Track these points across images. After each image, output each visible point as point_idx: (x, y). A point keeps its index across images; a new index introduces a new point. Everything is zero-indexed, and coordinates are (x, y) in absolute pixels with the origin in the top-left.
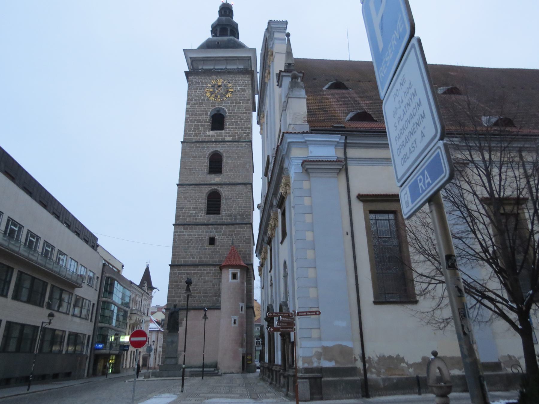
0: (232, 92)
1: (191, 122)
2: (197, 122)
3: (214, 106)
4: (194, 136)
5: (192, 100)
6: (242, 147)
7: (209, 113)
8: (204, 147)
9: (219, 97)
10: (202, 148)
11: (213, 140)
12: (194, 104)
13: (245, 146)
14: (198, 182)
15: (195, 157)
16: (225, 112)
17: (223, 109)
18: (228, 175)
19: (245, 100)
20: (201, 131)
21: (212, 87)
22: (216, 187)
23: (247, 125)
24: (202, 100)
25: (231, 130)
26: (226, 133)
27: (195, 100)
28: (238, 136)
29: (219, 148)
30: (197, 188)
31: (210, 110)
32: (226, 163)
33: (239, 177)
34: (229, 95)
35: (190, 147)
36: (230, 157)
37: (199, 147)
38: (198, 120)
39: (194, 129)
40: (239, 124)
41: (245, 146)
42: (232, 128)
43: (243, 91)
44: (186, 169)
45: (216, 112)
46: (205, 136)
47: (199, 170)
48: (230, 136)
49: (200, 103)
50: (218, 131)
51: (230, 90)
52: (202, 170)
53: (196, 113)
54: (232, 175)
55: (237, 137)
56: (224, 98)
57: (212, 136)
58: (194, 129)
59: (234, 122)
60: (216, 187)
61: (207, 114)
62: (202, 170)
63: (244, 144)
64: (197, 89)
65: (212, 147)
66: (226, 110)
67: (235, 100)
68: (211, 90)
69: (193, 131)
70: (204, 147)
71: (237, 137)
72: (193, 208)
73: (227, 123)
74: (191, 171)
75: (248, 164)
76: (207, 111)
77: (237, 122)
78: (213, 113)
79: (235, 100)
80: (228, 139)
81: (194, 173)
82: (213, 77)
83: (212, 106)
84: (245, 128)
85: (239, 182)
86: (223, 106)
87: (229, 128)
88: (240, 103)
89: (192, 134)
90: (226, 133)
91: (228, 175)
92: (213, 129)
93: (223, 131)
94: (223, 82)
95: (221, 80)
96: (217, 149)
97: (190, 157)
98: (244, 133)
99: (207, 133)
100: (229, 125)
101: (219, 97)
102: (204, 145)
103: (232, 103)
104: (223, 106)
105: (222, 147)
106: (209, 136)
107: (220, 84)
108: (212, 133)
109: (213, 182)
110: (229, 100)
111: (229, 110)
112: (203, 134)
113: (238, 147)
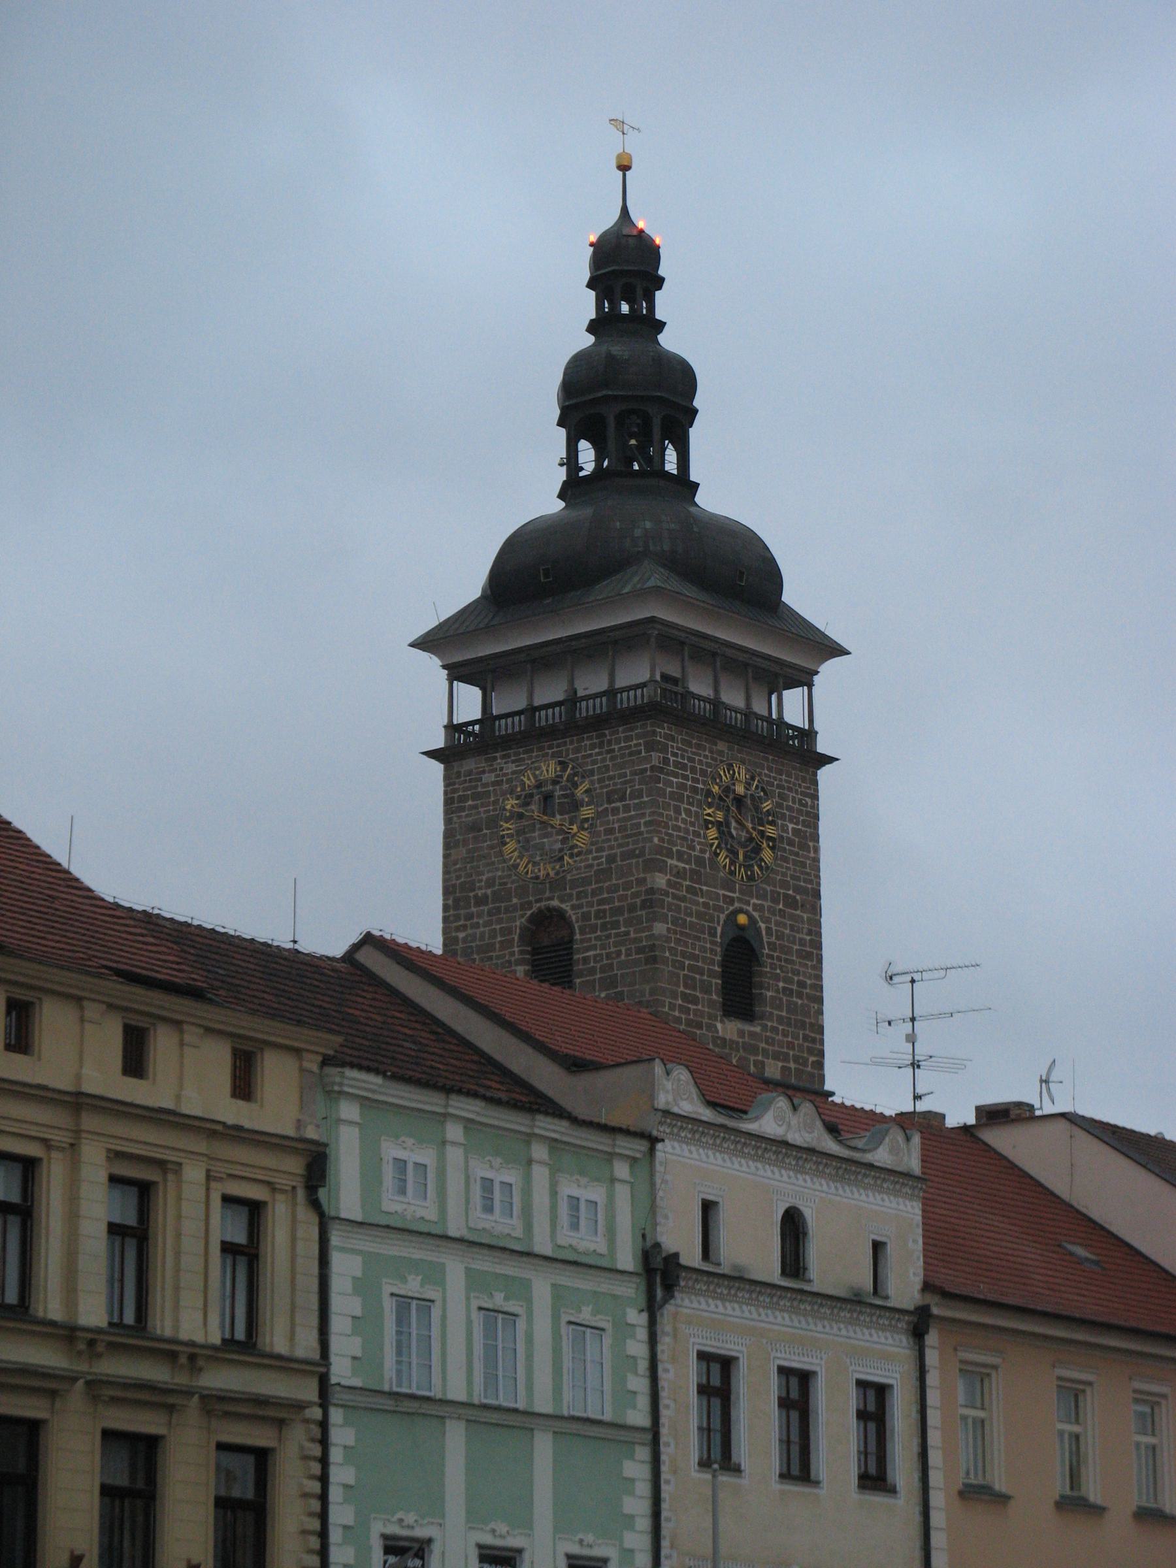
2: (692, 968)
3: (731, 901)
9: (741, 857)
27: (680, 856)
28: (796, 1059)
31: (722, 917)
42: (780, 1019)
48: (776, 1056)
50: (747, 1027)
51: (771, 831)
55: (792, 1065)
58: (685, 997)
66: (763, 926)
68: (720, 816)
71: (792, 1065)
82: (721, 746)
94: (748, 785)
98: (811, 1051)
99: (719, 1026)
103: (775, 901)
107: (740, 789)
108: (729, 1029)
111: (768, 929)
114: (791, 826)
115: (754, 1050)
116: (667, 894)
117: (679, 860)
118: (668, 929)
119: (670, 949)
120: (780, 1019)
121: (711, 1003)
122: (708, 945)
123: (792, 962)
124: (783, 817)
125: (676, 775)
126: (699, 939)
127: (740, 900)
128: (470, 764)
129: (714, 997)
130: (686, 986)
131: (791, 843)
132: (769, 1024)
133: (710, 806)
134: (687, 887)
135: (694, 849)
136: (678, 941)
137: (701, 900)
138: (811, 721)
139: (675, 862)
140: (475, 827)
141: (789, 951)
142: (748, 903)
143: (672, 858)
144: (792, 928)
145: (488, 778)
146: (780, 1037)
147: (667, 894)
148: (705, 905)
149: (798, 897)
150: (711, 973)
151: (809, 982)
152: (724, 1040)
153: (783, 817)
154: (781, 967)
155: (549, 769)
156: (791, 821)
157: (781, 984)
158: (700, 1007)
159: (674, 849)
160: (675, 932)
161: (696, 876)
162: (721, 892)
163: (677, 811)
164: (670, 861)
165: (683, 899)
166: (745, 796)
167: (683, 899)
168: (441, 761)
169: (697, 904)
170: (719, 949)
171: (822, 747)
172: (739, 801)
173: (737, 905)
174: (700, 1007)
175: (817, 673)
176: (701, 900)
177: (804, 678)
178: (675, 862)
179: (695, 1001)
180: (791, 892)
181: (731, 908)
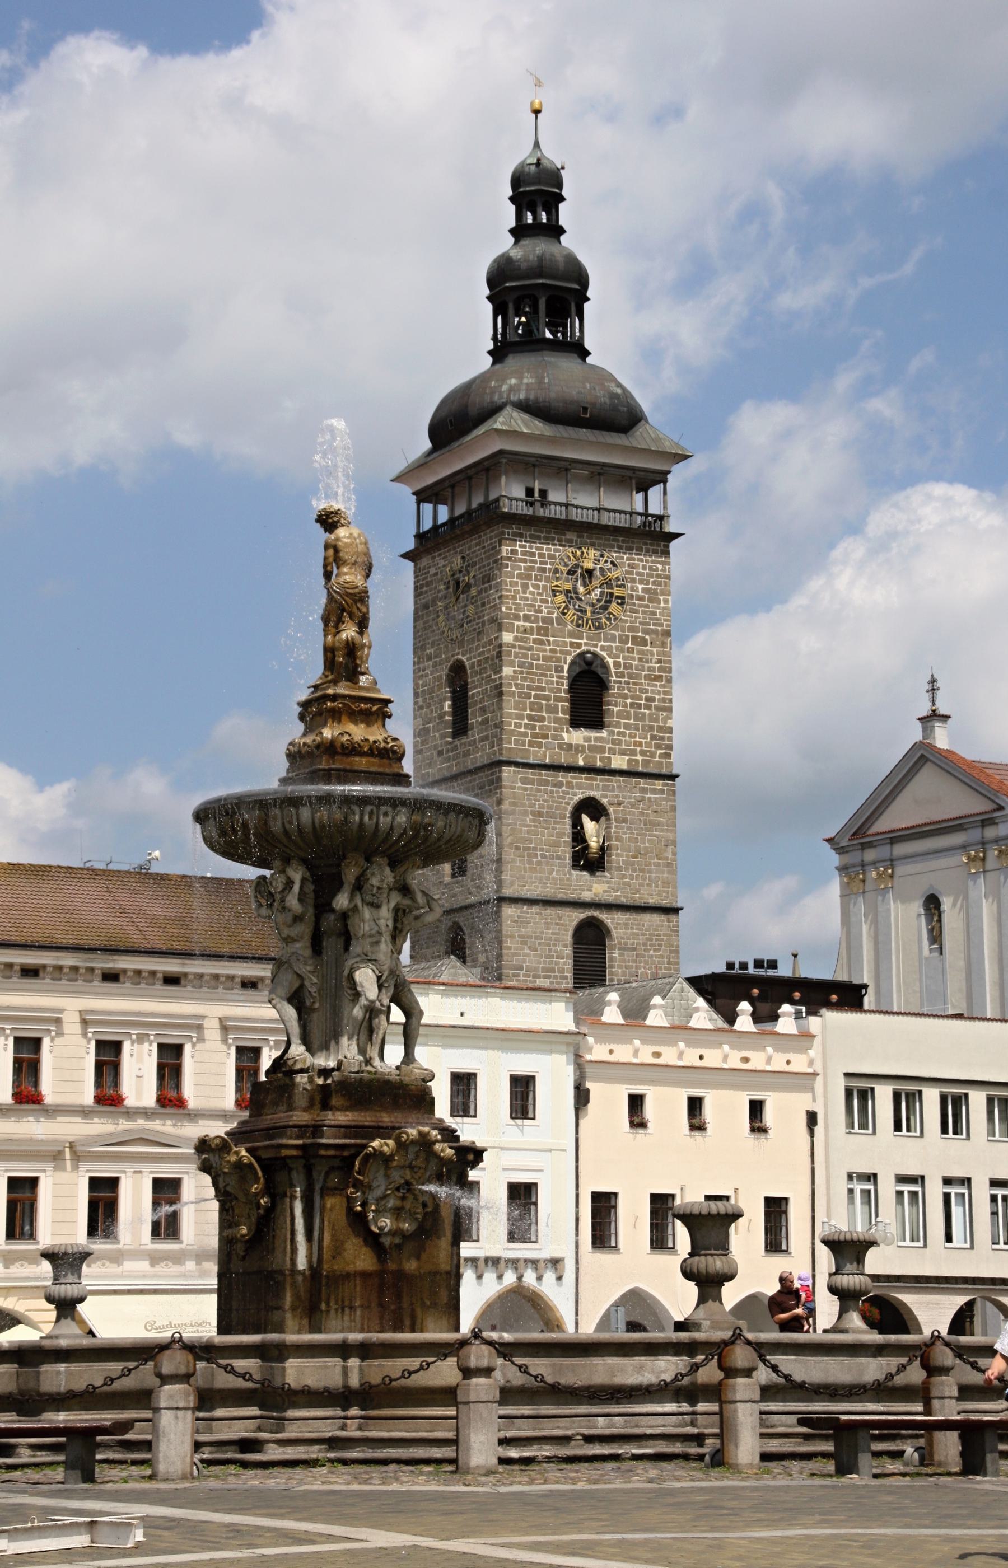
0: (623, 598)
1: (520, 695)
2: (536, 697)
3: (579, 646)
4: (531, 744)
5: (517, 618)
6: (654, 791)
7: (566, 667)
8: (560, 785)
9: (589, 614)
10: (555, 785)
11: (581, 763)
12: (525, 631)
13: (662, 791)
14: (549, 891)
15: (540, 814)
16: (605, 666)
17: (602, 659)
18: (624, 876)
19: (656, 632)
20: (548, 728)
21: (569, 573)
22: (596, 914)
23: (665, 721)
24: (545, 620)
25: (623, 734)
26: (614, 742)
27: (527, 618)
28: (643, 753)
29: (597, 789)
30: (549, 911)
31: (569, 659)
32: (618, 839)
33: (649, 885)
34: (614, 607)
35: (524, 781)
36: (625, 821)
37: (546, 783)
38: (539, 688)
39: (530, 718)
40: (644, 714)
41: (662, 791)
42: (627, 726)
43: (650, 600)
44: (517, 848)
45: (586, 668)
46: (560, 746)
47: (552, 857)
48: (622, 753)
49: (539, 628)
50: (593, 734)
51: (617, 591)
52: (559, 858)
53: (531, 665)
54: (631, 877)
55: (639, 758)
56: (604, 620)
57: (578, 749)
58: (530, 718)
59: (632, 705)
60: (596, 914)
61: (559, 670)
62: (559, 858)
63: (659, 784)
64: (529, 577)
65: (579, 786)
67: (631, 629)
68: (568, 586)
69: (526, 726)
70: (560, 785)
71: (639, 758)
72: (544, 970)
73: (614, 707)
74: (530, 856)
75: (670, 849)
76: (559, 660)
77: (639, 706)
78: (578, 670)
79: (631, 629)
80: (619, 762)
81: (539, 863)
83: (572, 644)
84: (661, 729)
85: (652, 901)
86: (603, 648)
87: (618, 725)
88: (644, 642)
89: (525, 735)
90: (614, 742)
91: (624, 876)
92: (576, 723)
93: (604, 734)
95: (592, 552)
96: (593, 793)
97: (525, 813)
99: (565, 735)
100: (620, 715)
101: (589, 614)
102: (561, 777)
103: (624, 640)
104: (603, 648)
105: (606, 788)
106: (570, 746)
107: (589, 564)
108: (577, 737)
109: (587, 896)
110: (616, 628)
111: (617, 665)
112: (555, 737)
113: (644, 791)
114: (640, 587)
115: (602, 750)
116: (514, 646)
117: (525, 621)
118: (515, 672)
119: (516, 685)
120: (627, 726)
121: (557, 720)
122: (555, 679)
123: (641, 684)
124: (633, 581)
125: (525, 561)
126: (546, 676)
127: (586, 644)
128: (424, 562)
129: (561, 715)
130: (531, 710)
131: (640, 598)
132: (616, 730)
133: (557, 579)
134: (534, 640)
135: (541, 612)
136: (524, 679)
137: (548, 648)
138: (665, 508)
139: (522, 623)
140: (426, 607)
141: (638, 676)
142: (596, 646)
143: (519, 620)
144: (640, 660)
145: (433, 571)
146: (627, 738)
147: (514, 646)
148: (551, 651)
149: (647, 637)
150: (557, 699)
151: (657, 697)
152: (570, 745)
153: (633, 581)
154: (629, 689)
155: (457, 563)
156: (641, 582)
157: (629, 701)
158: (546, 723)
159: (521, 614)
160: (522, 672)
161: (543, 631)
162: (568, 640)
163: (525, 587)
164: (516, 623)
165: (531, 649)
166: (594, 570)
167: (531, 649)
168: (412, 561)
169: (545, 651)
170: (565, 681)
171: (671, 527)
172: (590, 572)
173: (584, 648)
174: (546, 723)
175: (669, 472)
176: (548, 648)
177: (661, 478)
178: (522, 623)
179: (542, 719)
180: (640, 634)
181: (578, 651)
